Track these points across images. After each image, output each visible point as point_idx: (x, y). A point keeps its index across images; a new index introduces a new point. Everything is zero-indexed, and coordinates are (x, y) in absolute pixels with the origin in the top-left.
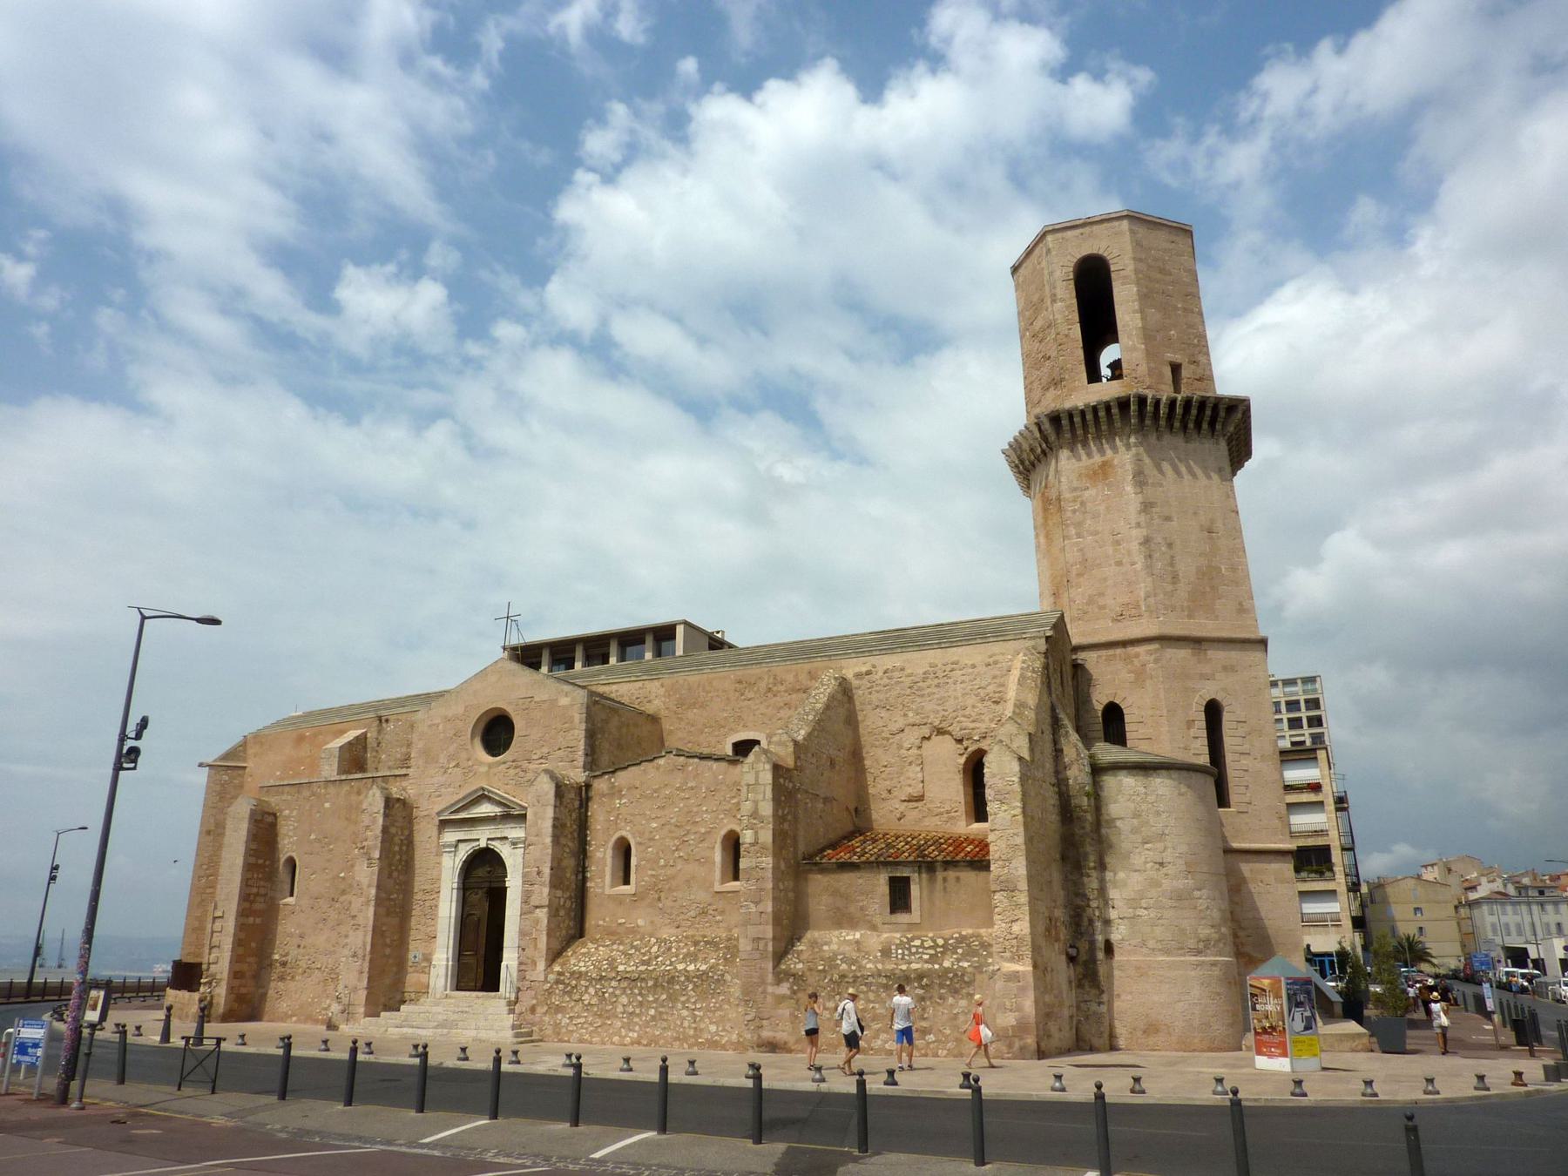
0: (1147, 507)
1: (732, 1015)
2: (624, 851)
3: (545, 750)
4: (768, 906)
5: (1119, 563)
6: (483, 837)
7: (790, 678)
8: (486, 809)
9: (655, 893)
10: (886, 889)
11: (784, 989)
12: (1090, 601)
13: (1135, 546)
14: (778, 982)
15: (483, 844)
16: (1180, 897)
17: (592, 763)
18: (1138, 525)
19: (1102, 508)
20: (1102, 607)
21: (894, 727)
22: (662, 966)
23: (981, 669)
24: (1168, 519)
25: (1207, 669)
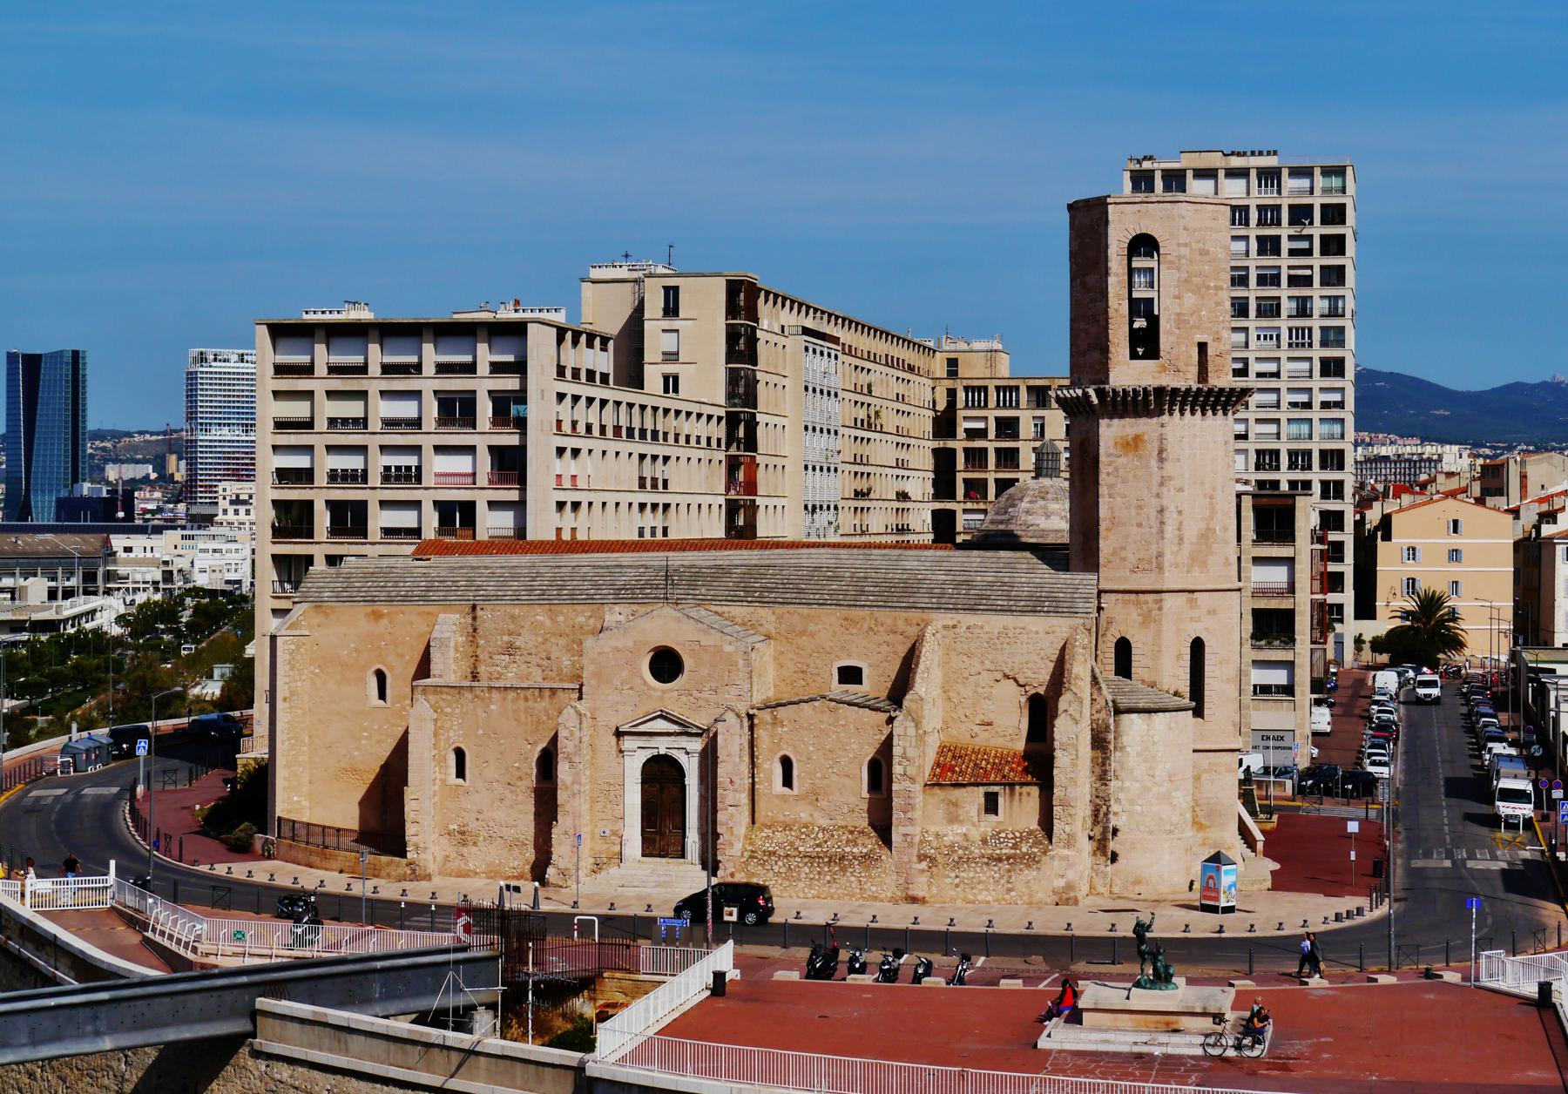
1: (888, 880)
3: (714, 685)
5: (1140, 525)
6: (662, 746)
7: (889, 621)
8: (661, 725)
9: (814, 796)
10: (982, 800)
11: (924, 865)
12: (1114, 553)
13: (1153, 513)
14: (920, 861)
15: (662, 752)
18: (1158, 496)
19: (1130, 476)
20: (1123, 559)
21: (973, 671)
22: (832, 847)
23: (1042, 635)
24: (1181, 490)
25: (1196, 613)
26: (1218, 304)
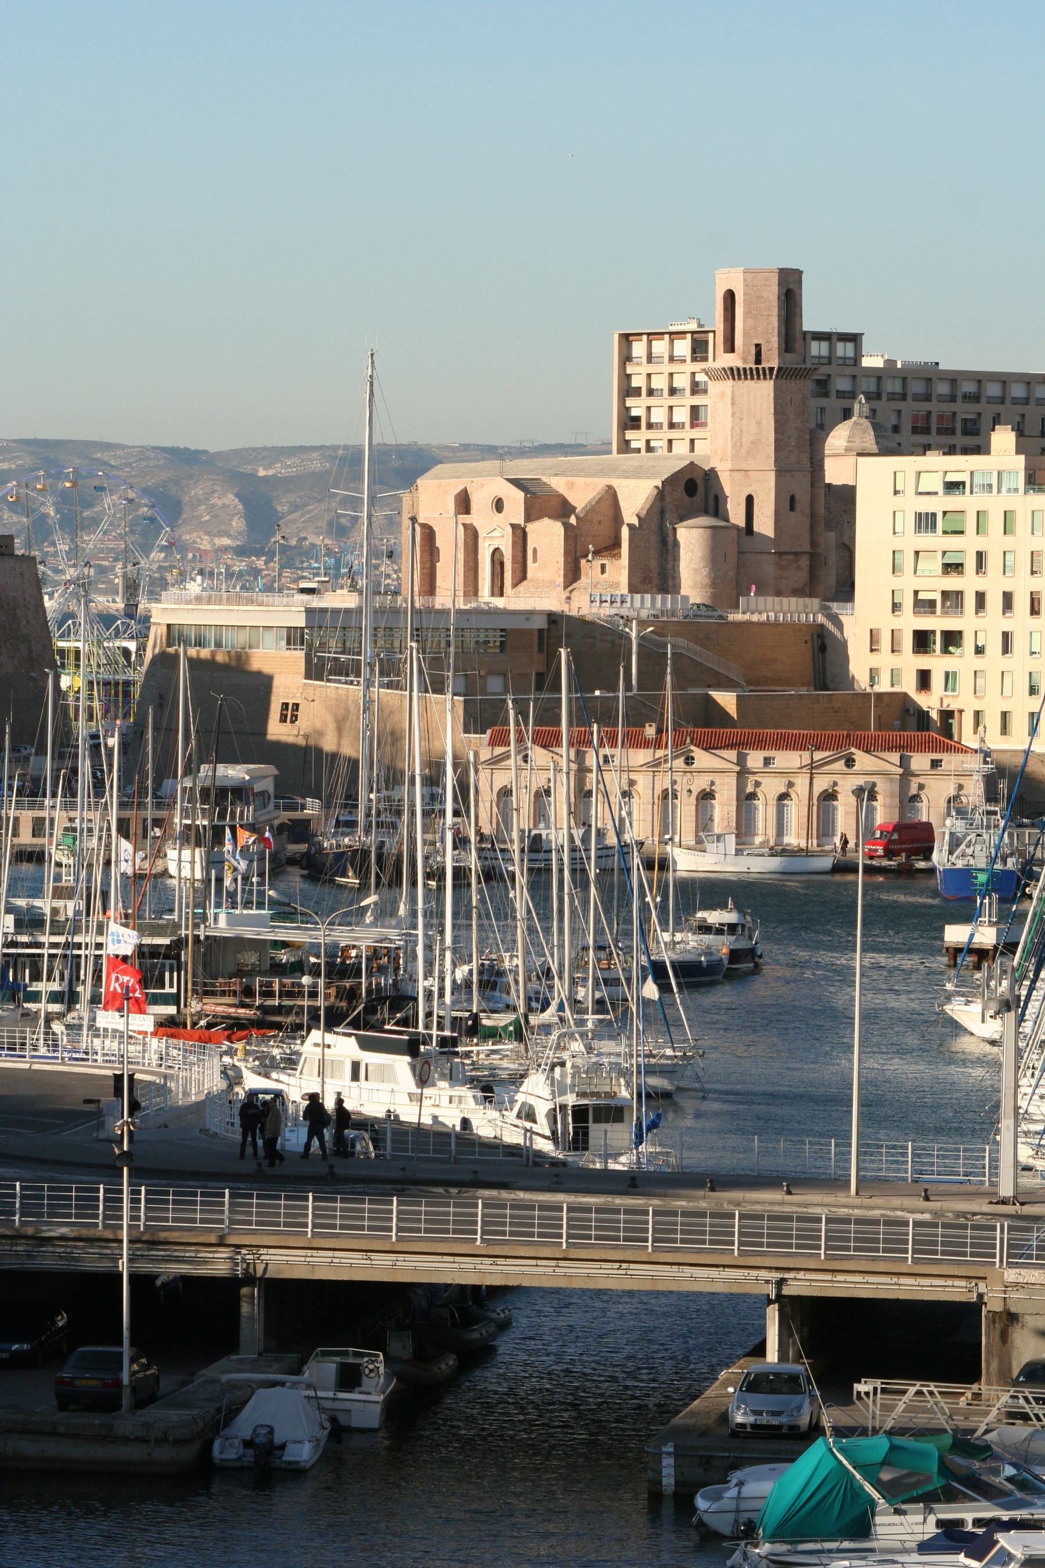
0: (733, 414)
2: (535, 550)
4: (562, 572)
16: (696, 570)
17: (529, 518)
26: (769, 324)
